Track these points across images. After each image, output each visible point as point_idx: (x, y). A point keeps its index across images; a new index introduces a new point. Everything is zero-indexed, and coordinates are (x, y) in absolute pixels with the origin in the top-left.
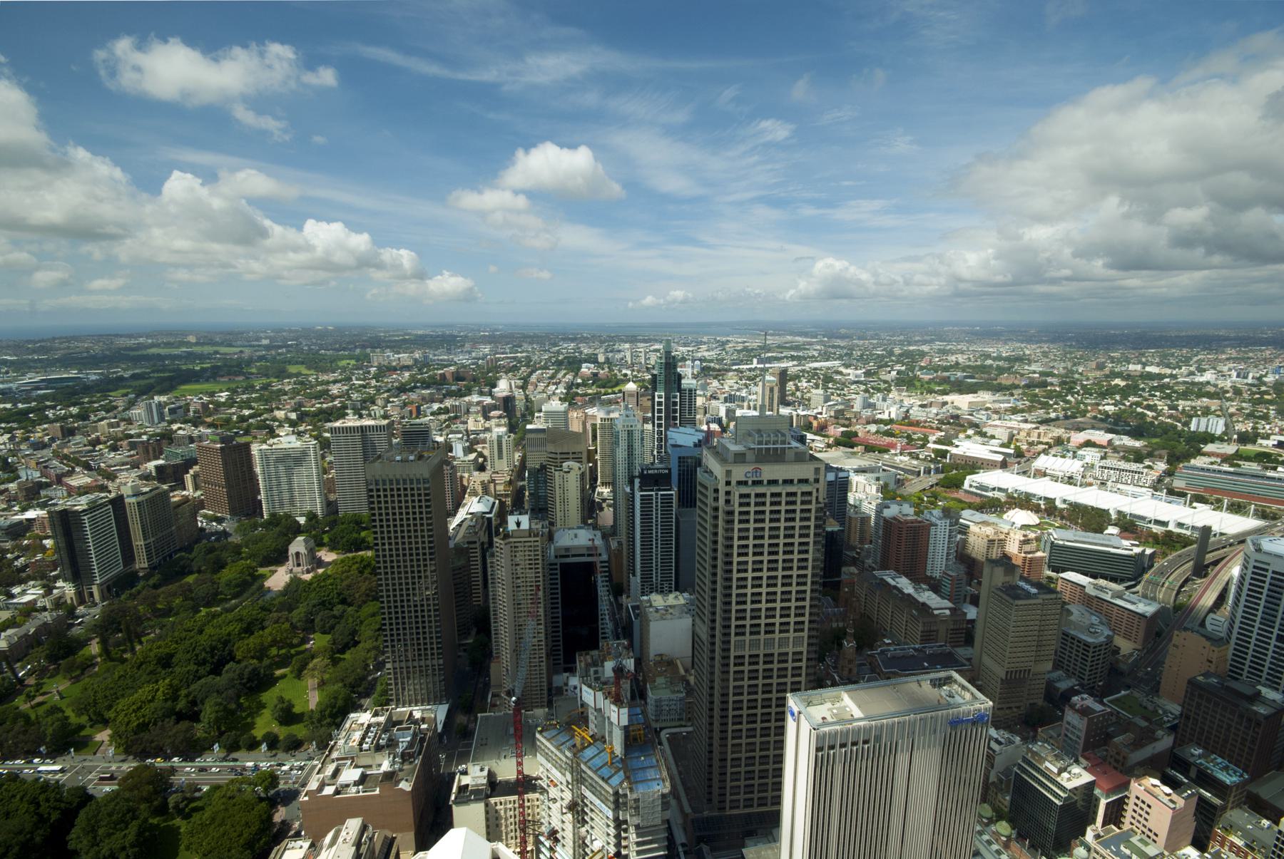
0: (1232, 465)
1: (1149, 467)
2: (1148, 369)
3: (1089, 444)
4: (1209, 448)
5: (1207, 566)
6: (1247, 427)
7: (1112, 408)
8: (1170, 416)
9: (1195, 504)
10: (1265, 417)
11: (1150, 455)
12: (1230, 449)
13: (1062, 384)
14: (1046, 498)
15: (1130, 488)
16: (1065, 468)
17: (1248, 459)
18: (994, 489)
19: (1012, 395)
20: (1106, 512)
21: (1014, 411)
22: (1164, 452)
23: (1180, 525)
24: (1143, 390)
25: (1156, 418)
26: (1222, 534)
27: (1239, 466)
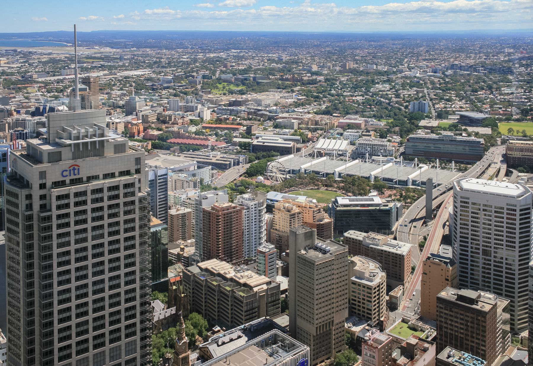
0: (438, 134)
1: (389, 141)
2: (379, 68)
3: (350, 126)
4: (422, 123)
5: (434, 210)
6: (440, 106)
7: (361, 98)
8: (397, 102)
9: (420, 165)
10: (448, 100)
11: (389, 131)
12: (435, 123)
13: (327, 80)
14: (327, 174)
15: (381, 158)
16: (336, 147)
17: (445, 129)
18: (289, 172)
19: (293, 91)
20: (368, 178)
21: (297, 104)
22: (397, 129)
23: (414, 182)
24: (378, 83)
25: (389, 104)
26: (439, 185)
27: (441, 134)
